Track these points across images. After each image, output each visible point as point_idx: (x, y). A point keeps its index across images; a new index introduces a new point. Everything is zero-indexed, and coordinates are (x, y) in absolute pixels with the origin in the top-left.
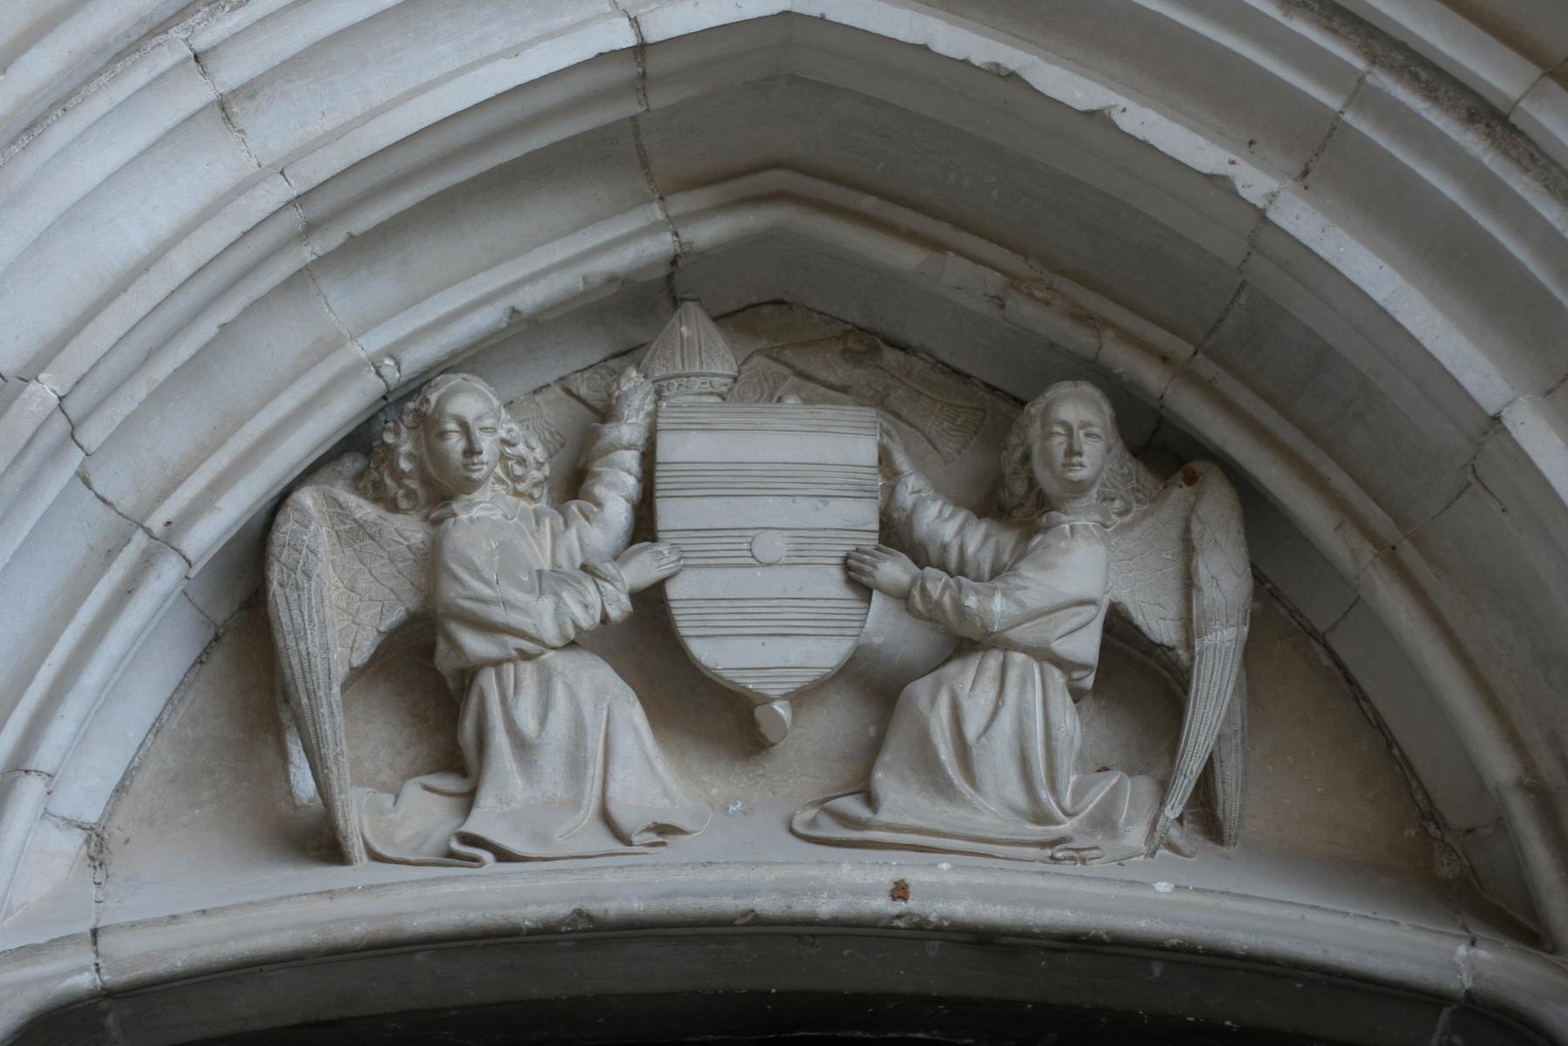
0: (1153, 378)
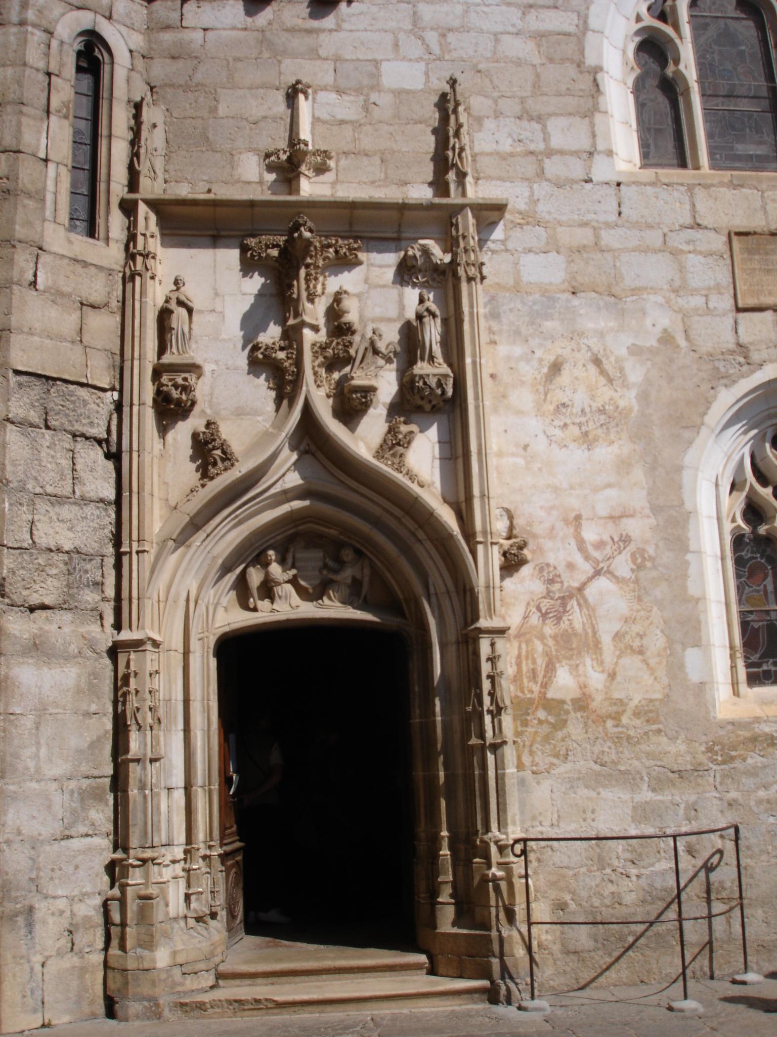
0: (358, 546)
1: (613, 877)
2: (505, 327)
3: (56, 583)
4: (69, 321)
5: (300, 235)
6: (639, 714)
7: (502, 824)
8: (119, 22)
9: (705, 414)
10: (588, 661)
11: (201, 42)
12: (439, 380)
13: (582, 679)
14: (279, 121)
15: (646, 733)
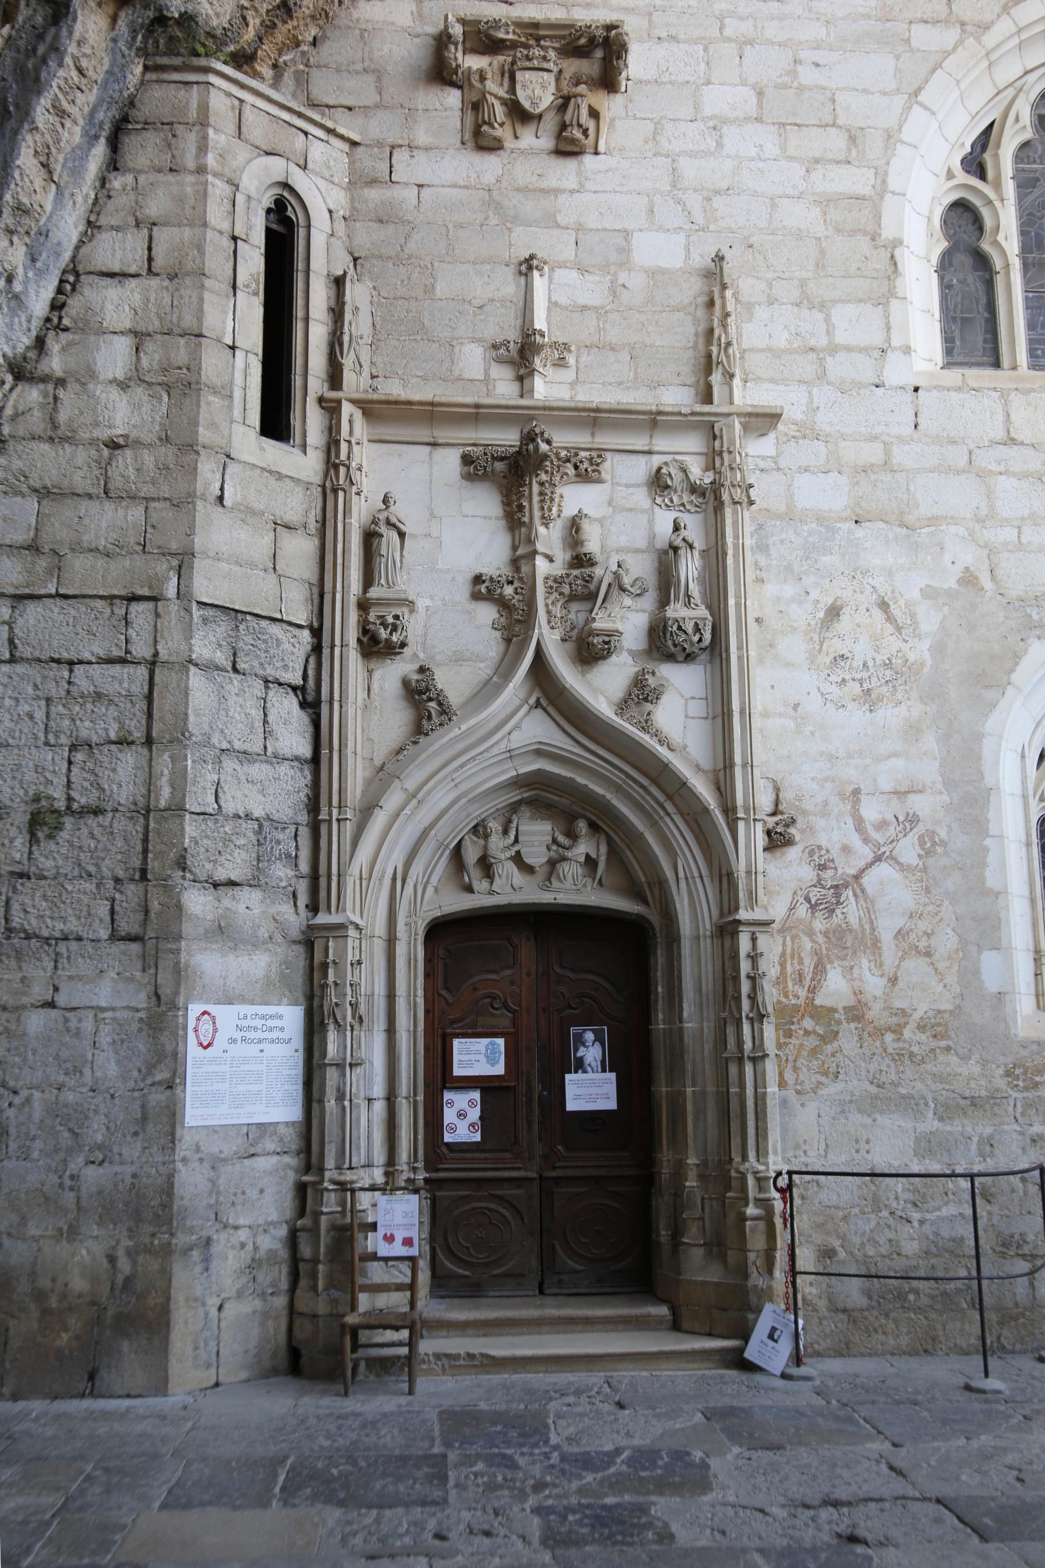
0: (594, 818)
1: (891, 1221)
2: (774, 562)
3: (244, 855)
4: (260, 545)
5: (537, 448)
6: (924, 1027)
7: (761, 1153)
8: (316, 174)
9: (1012, 671)
10: (865, 963)
11: (415, 202)
12: (696, 624)
13: (856, 984)
14: (509, 304)
15: (933, 1051)
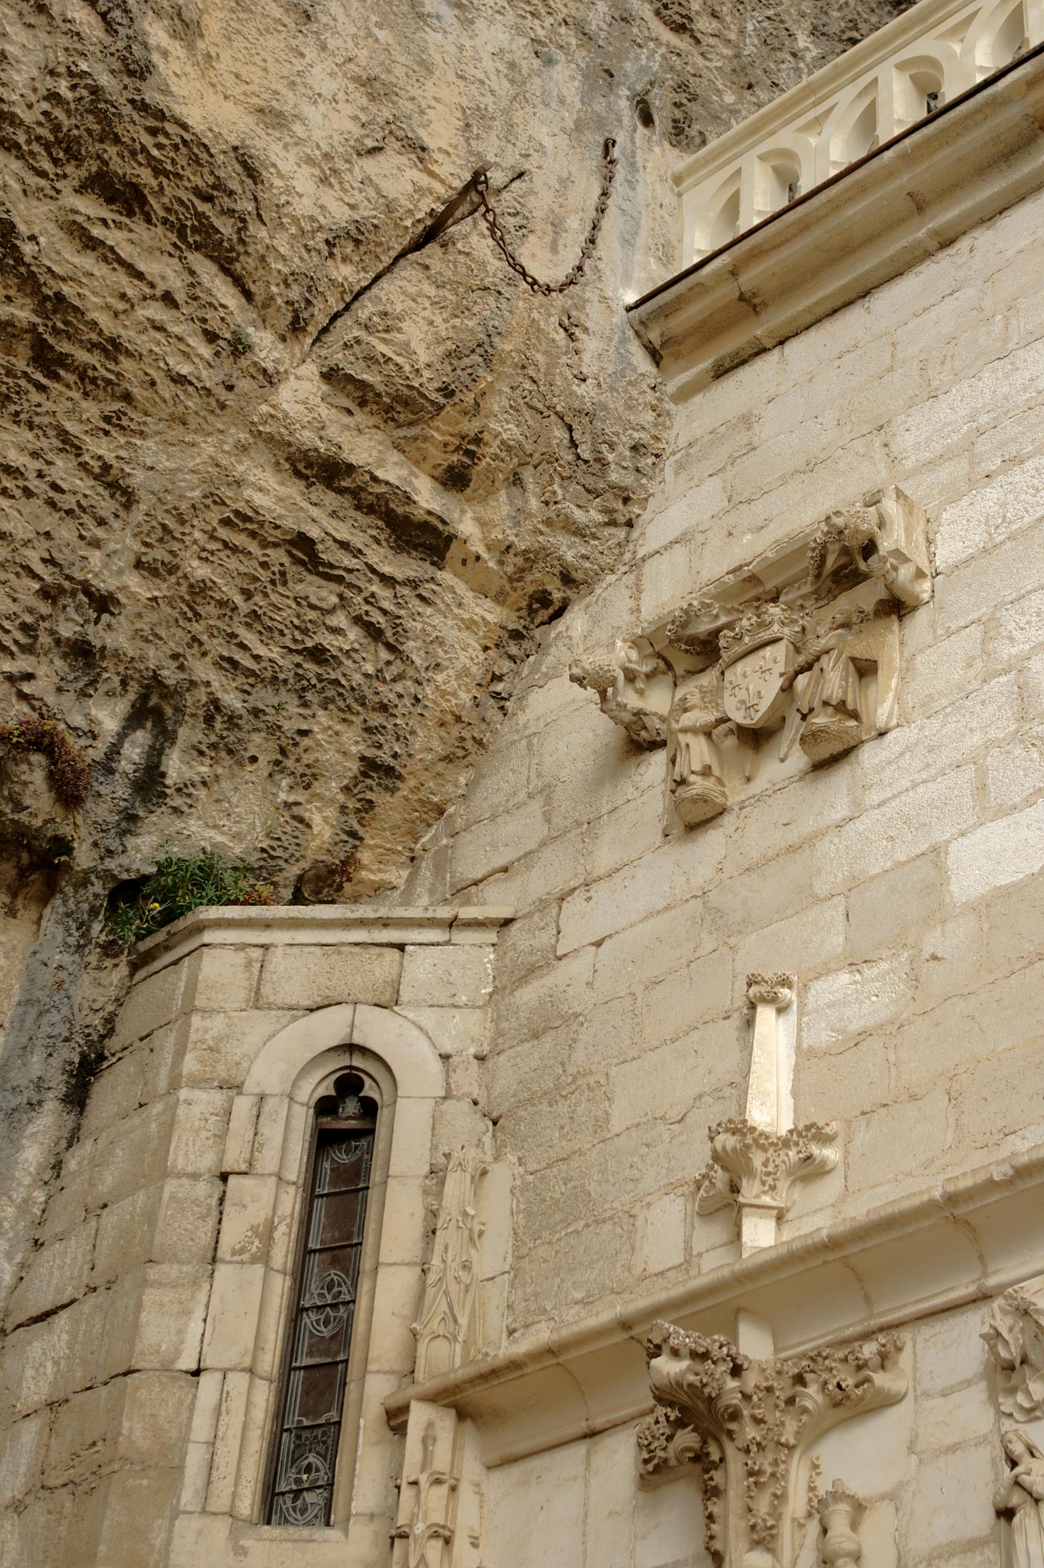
8: (417, 1004)
